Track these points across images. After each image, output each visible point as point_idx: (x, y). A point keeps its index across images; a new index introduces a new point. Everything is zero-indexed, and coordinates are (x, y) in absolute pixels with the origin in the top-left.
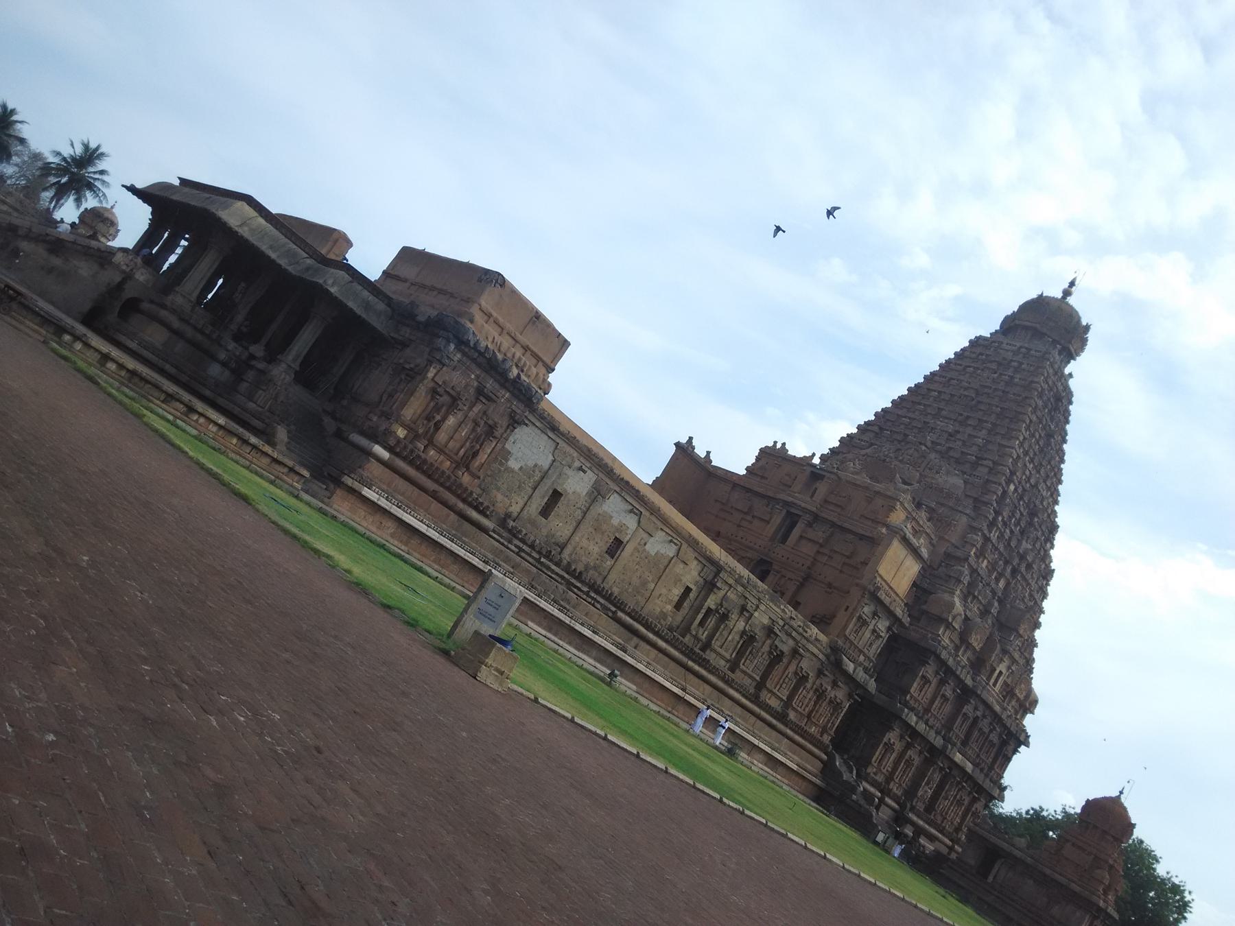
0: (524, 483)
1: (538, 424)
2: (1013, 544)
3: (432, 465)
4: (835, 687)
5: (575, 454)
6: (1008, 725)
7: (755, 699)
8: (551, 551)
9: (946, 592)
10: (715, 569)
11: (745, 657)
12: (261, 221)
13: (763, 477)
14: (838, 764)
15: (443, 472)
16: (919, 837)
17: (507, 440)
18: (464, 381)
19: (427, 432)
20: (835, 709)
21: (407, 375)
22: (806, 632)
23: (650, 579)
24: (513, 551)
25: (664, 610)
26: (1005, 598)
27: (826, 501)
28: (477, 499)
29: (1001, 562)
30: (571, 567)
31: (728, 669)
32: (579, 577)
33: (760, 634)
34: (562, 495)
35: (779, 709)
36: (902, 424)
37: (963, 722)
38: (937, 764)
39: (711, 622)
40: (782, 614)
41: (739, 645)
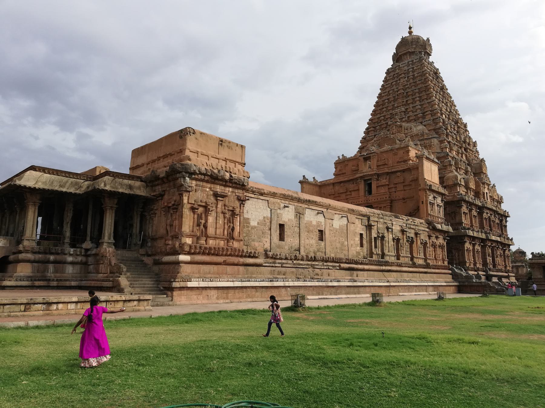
1: (253, 196)
2: (458, 139)
5: (279, 201)
6: (500, 212)
7: (414, 265)
14: (456, 271)
15: (223, 248)
16: (502, 280)
20: (442, 249)
21: (173, 209)
22: (415, 223)
23: (343, 240)
24: (279, 267)
25: (357, 251)
26: (469, 162)
27: (377, 166)
29: (459, 149)
31: (397, 260)
32: (315, 259)
33: (400, 235)
35: (425, 264)
36: (381, 120)
40: (403, 221)
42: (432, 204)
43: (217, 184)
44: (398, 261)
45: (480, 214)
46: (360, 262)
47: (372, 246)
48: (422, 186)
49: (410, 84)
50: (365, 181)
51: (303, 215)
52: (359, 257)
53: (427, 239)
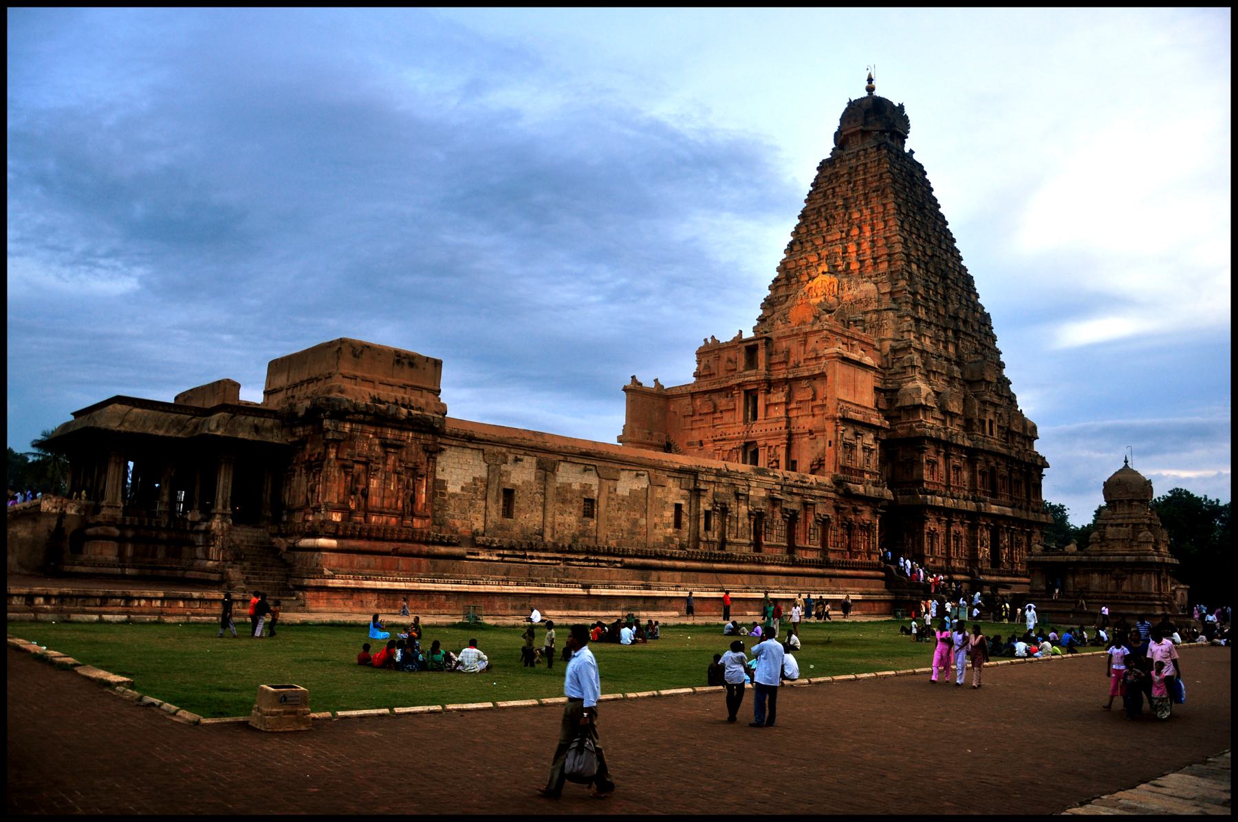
1: (455, 443)
2: (942, 312)
3: (378, 529)
5: (504, 450)
8: (531, 543)
9: (909, 382)
10: (692, 477)
12: (137, 410)
13: (710, 375)
15: (393, 530)
16: (997, 592)
17: (435, 472)
19: (358, 505)
22: (805, 482)
23: (638, 516)
25: (668, 535)
28: (437, 535)
30: (558, 546)
33: (763, 507)
35: (821, 559)
37: (983, 479)
38: (982, 525)
39: (715, 521)
41: (752, 527)
43: (388, 427)
44: (757, 554)
47: (699, 527)
48: (830, 411)
50: (747, 392)
52: (671, 545)
53: (831, 513)
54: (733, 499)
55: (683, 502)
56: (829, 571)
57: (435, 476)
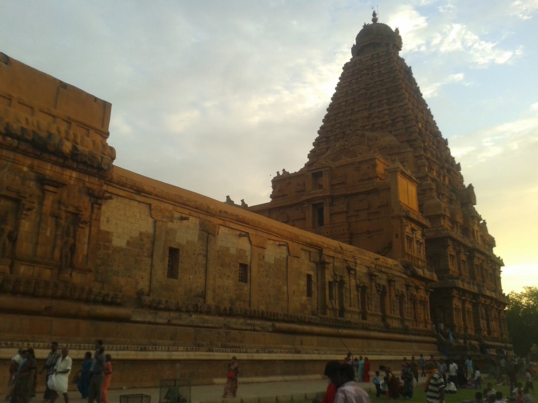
0: (138, 256)
1: (121, 193)
2: (439, 156)
4: (418, 291)
5: (171, 207)
7: (387, 329)
8: (196, 305)
11: (367, 304)
17: (98, 220)
18: (17, 178)
22: (387, 264)
23: (281, 283)
25: (303, 302)
27: (332, 185)
28: (100, 293)
34: (179, 249)
35: (400, 326)
41: (360, 297)
42: (410, 240)
45: (471, 258)
46: (307, 320)
47: (325, 296)
49: (375, 82)
50: (314, 206)
51: (214, 235)
53: (404, 291)
54: (346, 273)
55: (311, 273)
56: (407, 337)
57: (99, 227)
